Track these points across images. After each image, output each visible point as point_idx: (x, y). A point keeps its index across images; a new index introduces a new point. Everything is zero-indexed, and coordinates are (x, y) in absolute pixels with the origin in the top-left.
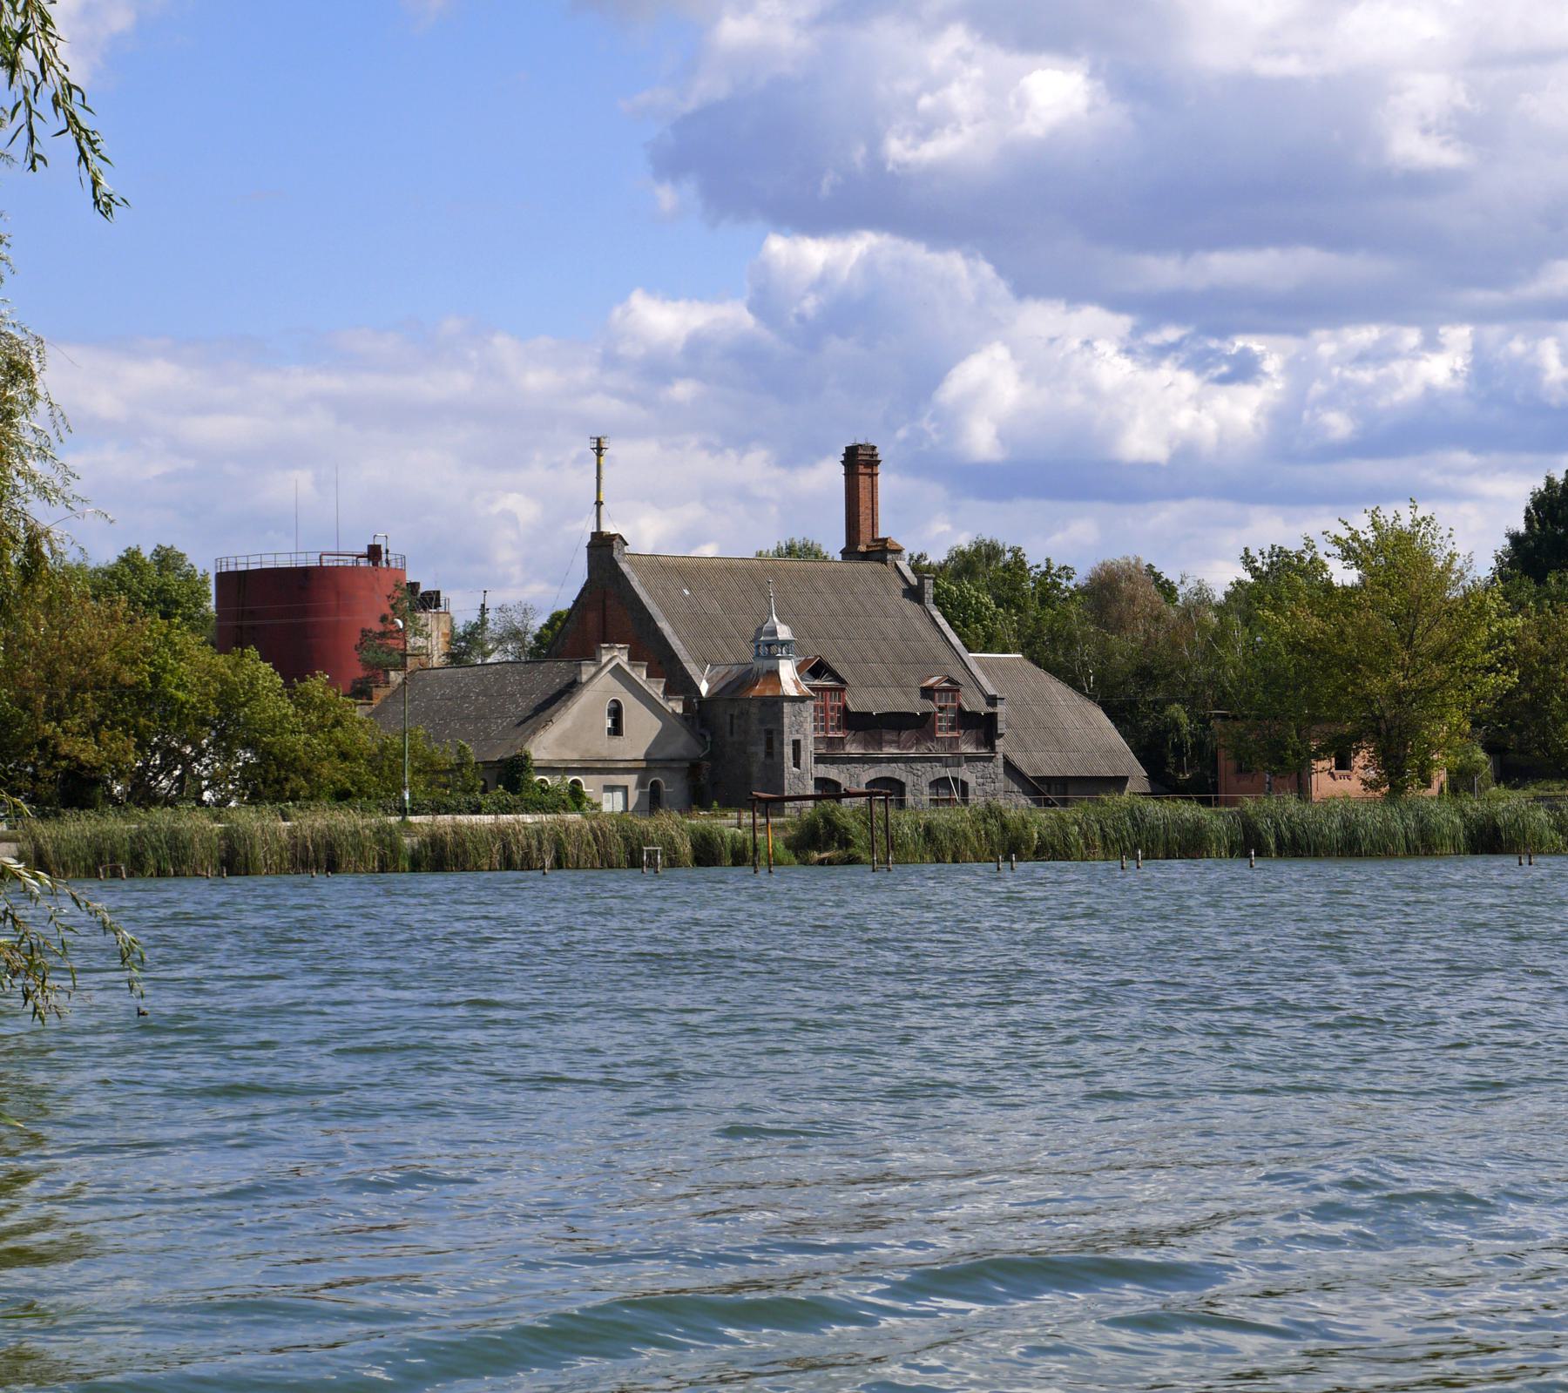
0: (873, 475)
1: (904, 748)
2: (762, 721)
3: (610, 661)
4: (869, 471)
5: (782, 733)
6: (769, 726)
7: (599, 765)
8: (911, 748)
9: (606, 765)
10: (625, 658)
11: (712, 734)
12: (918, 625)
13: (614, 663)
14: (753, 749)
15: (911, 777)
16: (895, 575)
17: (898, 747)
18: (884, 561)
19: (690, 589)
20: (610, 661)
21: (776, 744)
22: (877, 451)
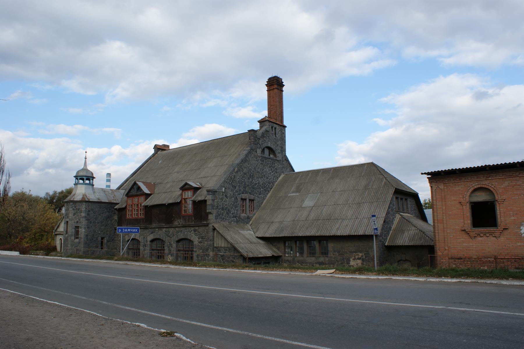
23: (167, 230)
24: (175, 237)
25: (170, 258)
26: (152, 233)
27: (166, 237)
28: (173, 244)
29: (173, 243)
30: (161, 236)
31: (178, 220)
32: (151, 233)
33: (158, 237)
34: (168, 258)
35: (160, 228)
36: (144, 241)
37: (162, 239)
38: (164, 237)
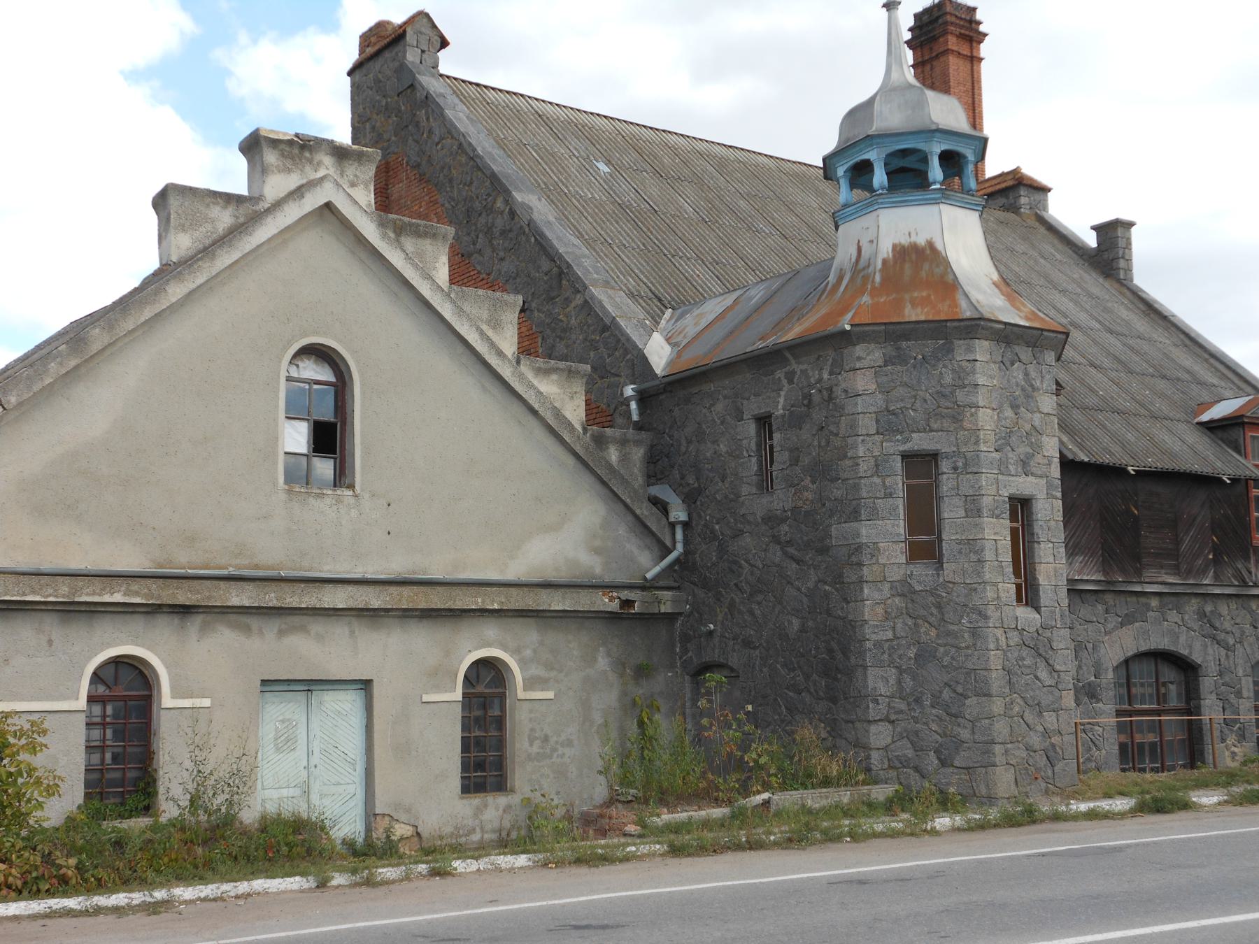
0: (974, 60)
1: (1189, 573)
2: (889, 424)
3: (298, 193)
4: (965, 50)
5: (969, 466)
6: (919, 442)
7: (238, 597)
8: (1203, 572)
9: (271, 598)
10: (366, 196)
11: (690, 499)
12: (1124, 313)
13: (312, 201)
14: (866, 531)
15: (1214, 651)
16: (1042, 230)
17: (1176, 570)
18: (1014, 209)
19: (608, 162)
20: (298, 193)
21: (951, 513)
22: (979, 16)
23: (1208, 608)
24: (1251, 645)
25: (1234, 749)
26: (1127, 620)
27: (1206, 646)
28: (1243, 682)
29: (1240, 673)
30: (1182, 639)
31: (1240, 566)
32: (1122, 625)
33: (1164, 643)
34: (1227, 753)
35: (1172, 598)
36: (1080, 667)
37: (1185, 652)
38: (1197, 645)
